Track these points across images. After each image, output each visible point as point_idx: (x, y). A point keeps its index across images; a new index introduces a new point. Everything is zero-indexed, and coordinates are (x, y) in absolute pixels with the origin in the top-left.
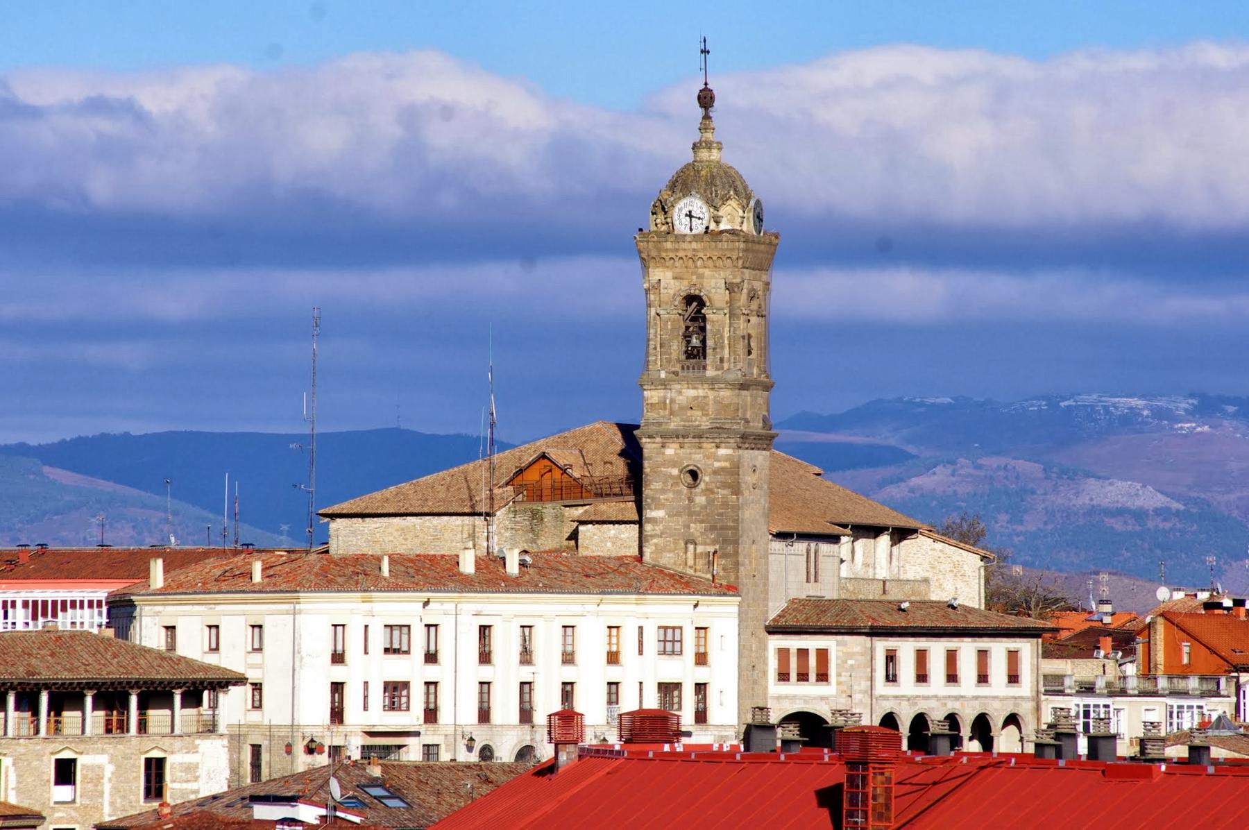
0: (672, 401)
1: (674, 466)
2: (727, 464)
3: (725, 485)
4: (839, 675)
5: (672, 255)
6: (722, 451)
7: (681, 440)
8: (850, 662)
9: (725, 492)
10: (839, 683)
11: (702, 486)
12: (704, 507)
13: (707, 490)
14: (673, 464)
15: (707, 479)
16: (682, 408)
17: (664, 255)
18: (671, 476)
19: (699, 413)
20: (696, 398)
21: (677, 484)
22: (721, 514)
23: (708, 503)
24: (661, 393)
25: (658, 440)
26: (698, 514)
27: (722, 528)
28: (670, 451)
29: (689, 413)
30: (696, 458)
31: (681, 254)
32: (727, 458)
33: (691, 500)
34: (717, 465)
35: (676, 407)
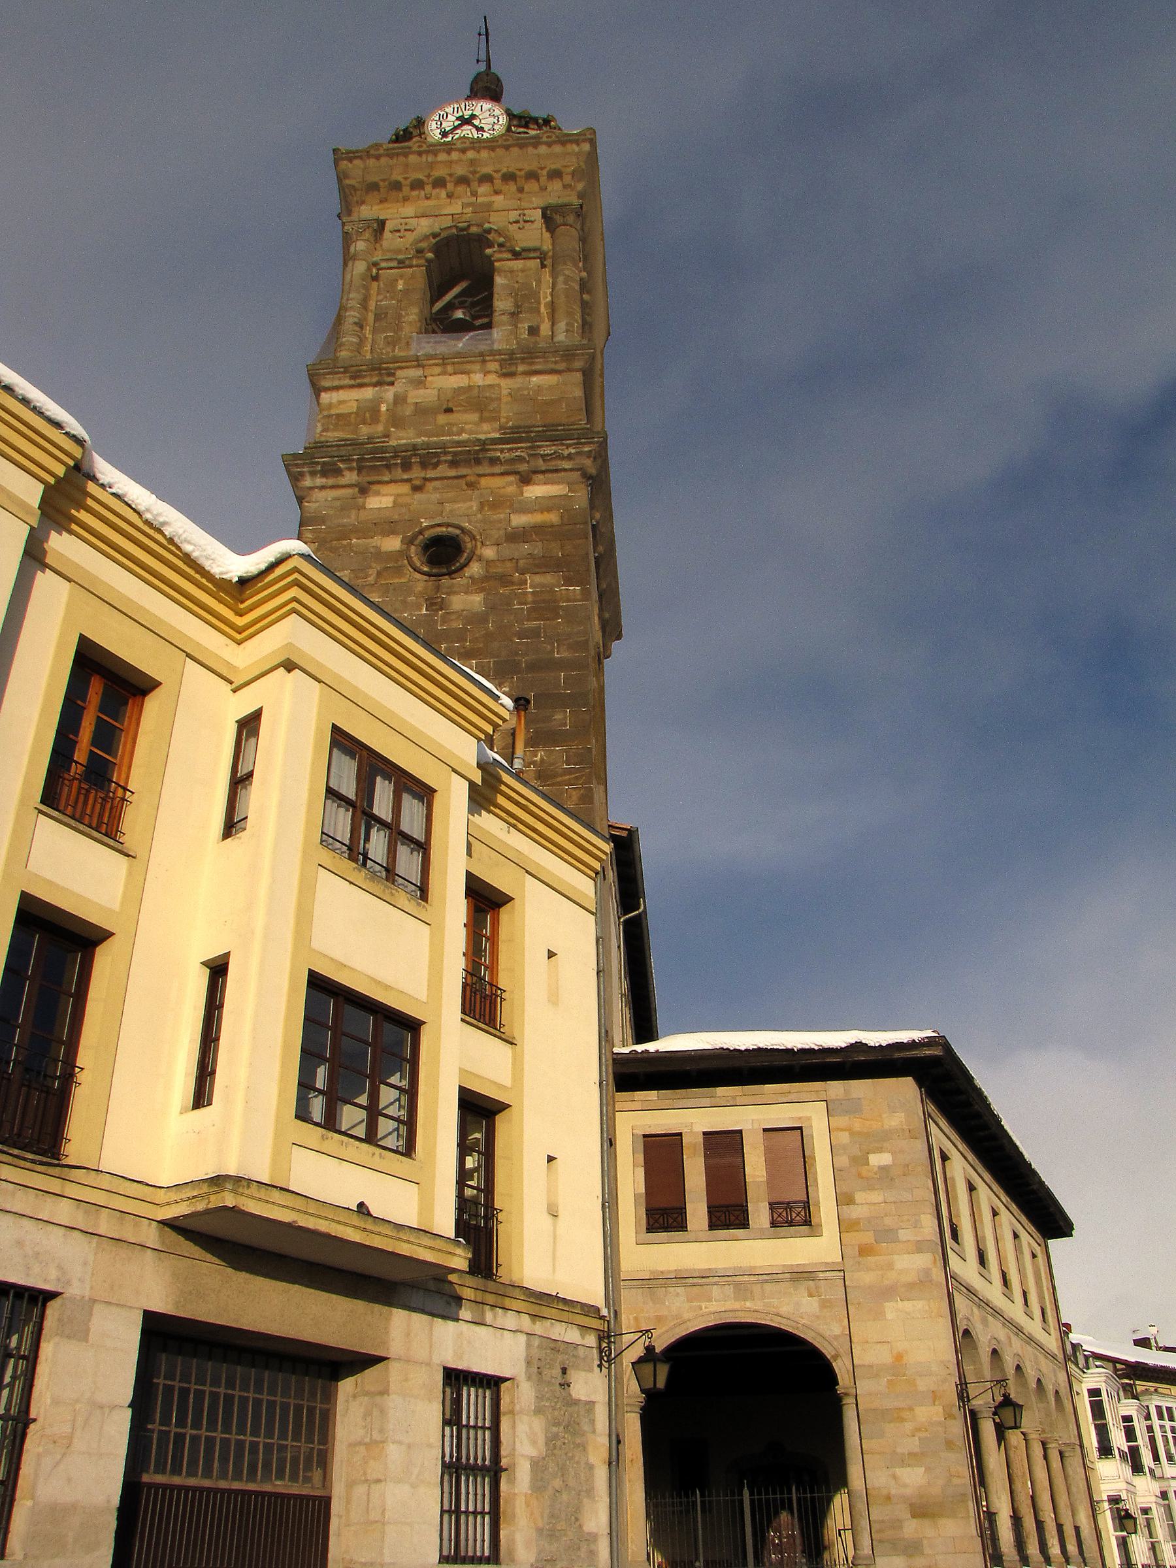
0: (399, 400)
1: (393, 532)
2: (553, 518)
3: (542, 564)
4: (844, 1199)
6: (535, 491)
7: (416, 473)
8: (877, 1160)
9: (548, 579)
10: (845, 1226)
11: (475, 569)
12: (478, 619)
13: (486, 578)
14: (388, 526)
16: (422, 411)
18: (378, 555)
19: (475, 417)
20: (458, 391)
21: (398, 571)
22: (535, 633)
23: (492, 607)
24: (368, 393)
25: (350, 477)
26: (460, 636)
27: (533, 667)
28: (380, 501)
29: (442, 419)
32: (545, 505)
33: (435, 604)
35: (409, 411)
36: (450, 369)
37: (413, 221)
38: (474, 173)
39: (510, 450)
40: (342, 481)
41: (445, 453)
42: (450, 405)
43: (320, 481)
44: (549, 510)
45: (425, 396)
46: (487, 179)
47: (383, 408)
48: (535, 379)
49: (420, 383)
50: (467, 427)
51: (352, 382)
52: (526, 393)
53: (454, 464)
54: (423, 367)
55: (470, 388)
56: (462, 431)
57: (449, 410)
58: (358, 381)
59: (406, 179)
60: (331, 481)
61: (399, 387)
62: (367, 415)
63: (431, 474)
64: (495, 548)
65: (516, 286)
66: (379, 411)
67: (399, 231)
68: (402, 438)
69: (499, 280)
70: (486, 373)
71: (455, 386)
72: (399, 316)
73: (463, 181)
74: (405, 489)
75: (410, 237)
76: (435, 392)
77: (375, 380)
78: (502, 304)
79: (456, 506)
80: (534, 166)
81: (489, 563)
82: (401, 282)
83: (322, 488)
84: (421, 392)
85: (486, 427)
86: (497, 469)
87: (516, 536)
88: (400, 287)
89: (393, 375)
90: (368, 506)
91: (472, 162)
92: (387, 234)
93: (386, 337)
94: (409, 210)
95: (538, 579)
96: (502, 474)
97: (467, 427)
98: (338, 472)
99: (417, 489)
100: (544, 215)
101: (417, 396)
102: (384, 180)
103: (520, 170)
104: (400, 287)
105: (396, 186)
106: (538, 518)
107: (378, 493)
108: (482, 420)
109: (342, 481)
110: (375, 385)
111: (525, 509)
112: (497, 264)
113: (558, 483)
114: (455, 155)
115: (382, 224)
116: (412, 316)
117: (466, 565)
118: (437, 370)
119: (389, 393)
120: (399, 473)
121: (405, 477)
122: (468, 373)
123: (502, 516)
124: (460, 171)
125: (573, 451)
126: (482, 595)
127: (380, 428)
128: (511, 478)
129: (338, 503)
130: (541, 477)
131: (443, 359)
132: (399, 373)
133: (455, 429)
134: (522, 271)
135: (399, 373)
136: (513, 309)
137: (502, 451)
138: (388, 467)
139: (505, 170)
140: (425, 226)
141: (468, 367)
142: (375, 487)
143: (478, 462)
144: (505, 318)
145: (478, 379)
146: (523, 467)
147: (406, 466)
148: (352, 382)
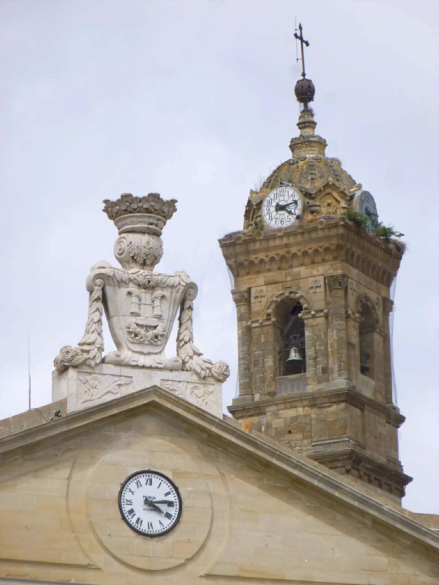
5: (262, 256)
17: (252, 257)
19: (300, 436)
31: (272, 254)
36: (288, 405)
38: (288, 253)
42: (290, 429)
52: (322, 416)
54: (277, 405)
55: (297, 417)
57: (290, 432)
65: (315, 337)
70: (304, 407)
71: (291, 416)
72: (264, 363)
76: (283, 420)
82: (263, 336)
84: (277, 421)
85: (306, 442)
88: (263, 341)
91: (287, 246)
93: (260, 378)
94: (261, 280)
108: (304, 438)
112: (305, 321)
118: (282, 406)
122: (295, 407)
124: (282, 252)
131: (284, 400)
135: (267, 409)
141: (296, 404)
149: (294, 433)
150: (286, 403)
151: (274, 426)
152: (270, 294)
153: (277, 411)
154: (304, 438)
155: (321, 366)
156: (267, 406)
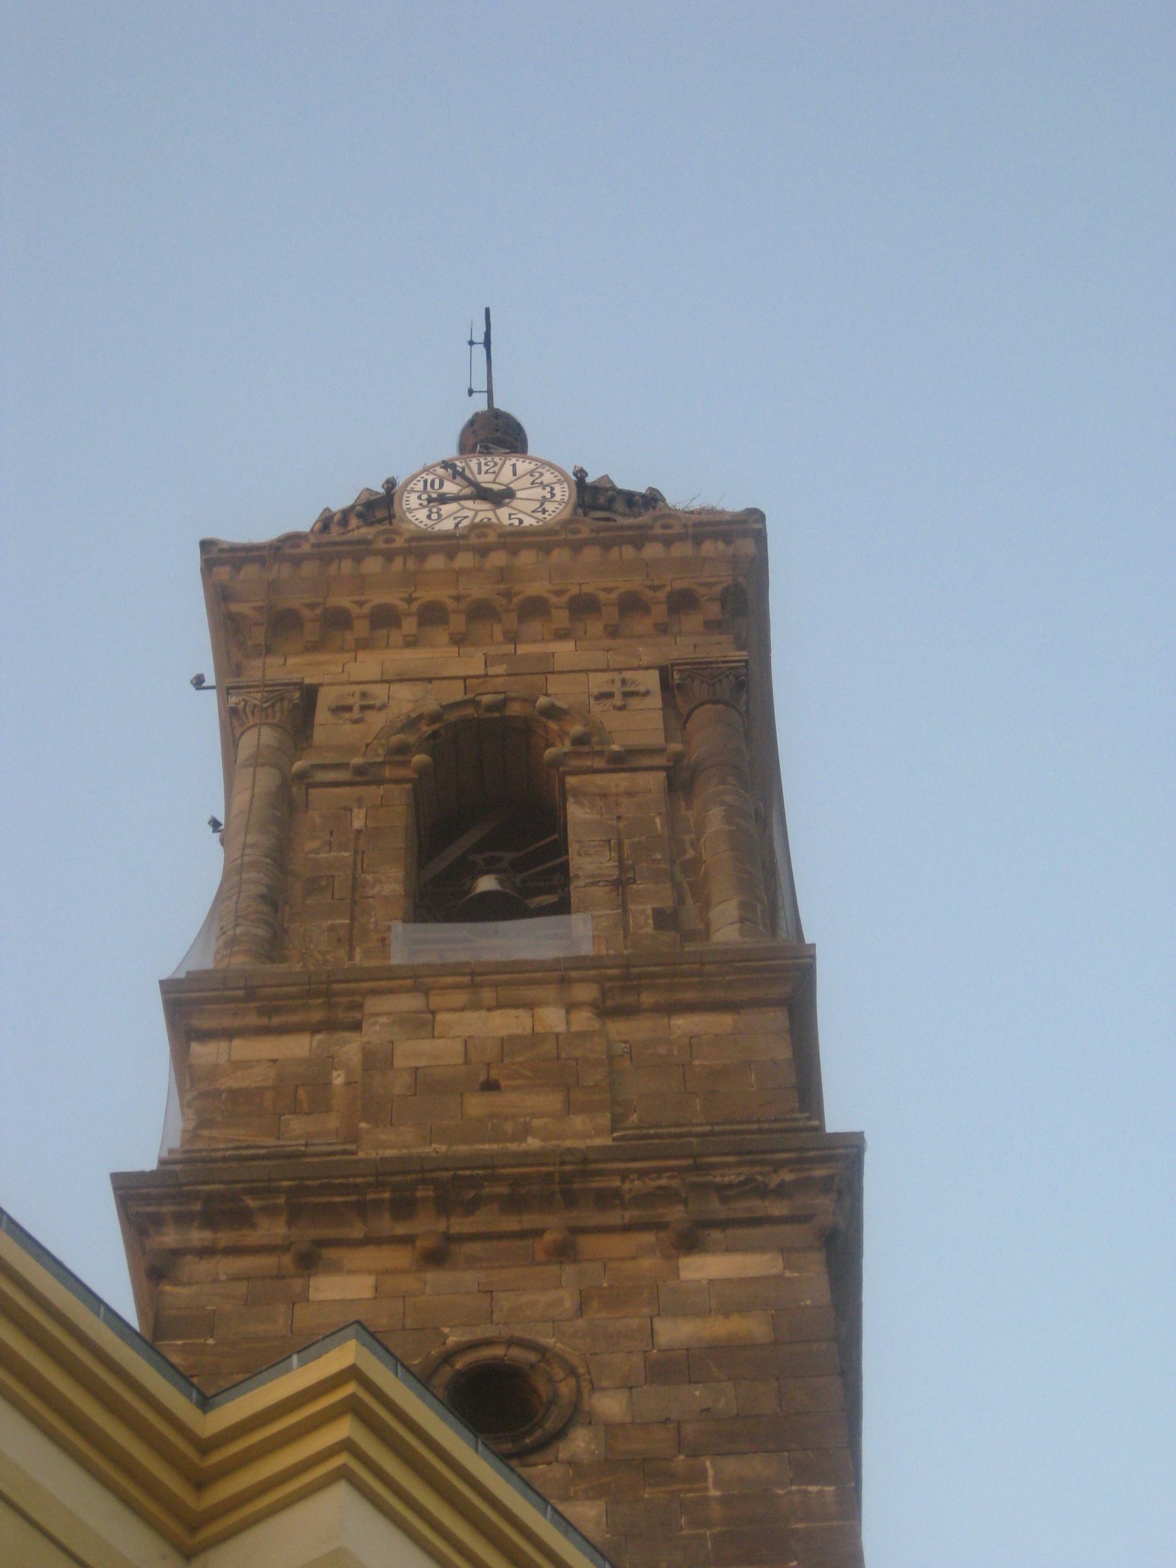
0: (376, 1061)
2: (752, 1327)
11: (580, 1443)
15: (610, 1405)
16: (427, 1084)
17: (344, 601)
19: (551, 1101)
24: (298, 1047)
25: (273, 1230)
29: (477, 1105)
30: (530, 1306)
32: (731, 1298)
34: (674, 1332)
35: (400, 1085)
36: (487, 995)
37: (379, 691)
38: (508, 595)
39: (643, 1173)
40: (253, 1237)
41: (495, 1179)
42: (495, 1074)
43: (198, 1236)
44: (742, 1309)
45: (438, 1051)
46: (535, 608)
47: (338, 1078)
48: (681, 1023)
49: (422, 1024)
50: (537, 1123)
51: (264, 1021)
52: (662, 1050)
53: (514, 1203)
54: (426, 991)
55: (535, 1038)
56: (526, 1131)
57: (491, 1086)
58: (276, 1020)
59: (361, 604)
60: (225, 1238)
61: (374, 1033)
62: (302, 1093)
63: (459, 1225)
64: (623, 1395)
66: (329, 1084)
67: (349, 709)
68: (389, 1143)
69: (577, 813)
70: (571, 1007)
71: (504, 1033)
72: (355, 886)
73: (481, 612)
74: (400, 1257)
75: (377, 721)
76: (459, 1046)
77: (317, 1016)
78: (588, 861)
79: (524, 1299)
80: (635, 583)
81: (610, 1428)
83: (206, 1252)
84: (426, 1045)
85: (579, 1122)
86: (614, 1217)
87: (669, 1369)
89: (360, 1007)
90: (313, 1295)
91: (503, 574)
92: (322, 715)
93: (332, 928)
94: (367, 666)
95: (732, 1467)
96: (627, 1228)
97: (537, 1123)
98: (244, 1218)
99: (435, 1258)
100: (666, 684)
101: (414, 1052)
102: (312, 606)
103: (609, 590)
104: (358, 824)
105: (338, 620)
106: (719, 1328)
107: (336, 1268)
108: (570, 1108)
109: (253, 1237)
110: (314, 1029)
111: (682, 1310)
112: (571, 781)
113: (761, 1249)
114: (464, 560)
115: (310, 694)
116: (390, 881)
117: (560, 1434)
118: (460, 998)
119: (351, 1048)
120: (386, 1225)
121: (401, 1230)
122: (530, 1006)
123: (635, 1323)
124: (478, 590)
125: (789, 1177)
126: (601, 1504)
127: (332, 1122)
128: (648, 1238)
129: (242, 1288)
130: (716, 1234)
131: (473, 974)
132: (371, 1004)
133: (509, 1127)
134: (629, 794)
135: (371, 1004)
136: (615, 874)
137: (624, 1175)
138: (362, 1209)
139: (575, 590)
140: (405, 700)
142: (330, 1253)
143: (570, 1200)
144: (599, 892)
145: (552, 1018)
146: (675, 1214)
147: (404, 1207)
148: (264, 1021)
149: (515, 1089)
150: (482, 985)
151: (399, 1063)
152: (406, 708)
153: (430, 1016)
154: (570, 1108)
155: (649, 908)
156: (374, 992)
